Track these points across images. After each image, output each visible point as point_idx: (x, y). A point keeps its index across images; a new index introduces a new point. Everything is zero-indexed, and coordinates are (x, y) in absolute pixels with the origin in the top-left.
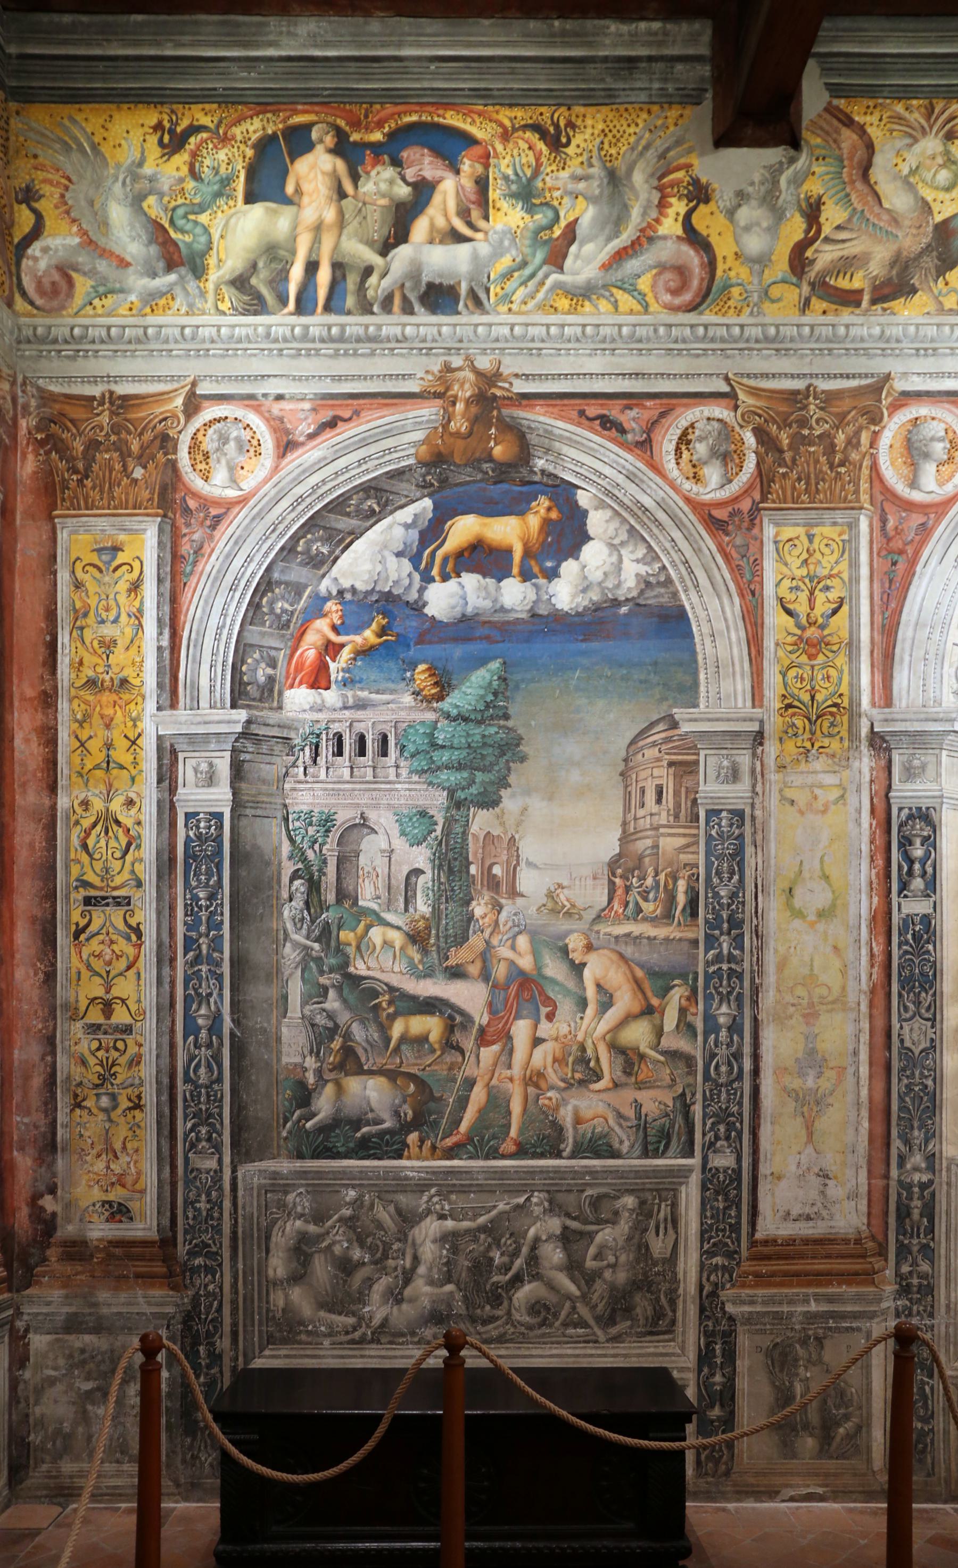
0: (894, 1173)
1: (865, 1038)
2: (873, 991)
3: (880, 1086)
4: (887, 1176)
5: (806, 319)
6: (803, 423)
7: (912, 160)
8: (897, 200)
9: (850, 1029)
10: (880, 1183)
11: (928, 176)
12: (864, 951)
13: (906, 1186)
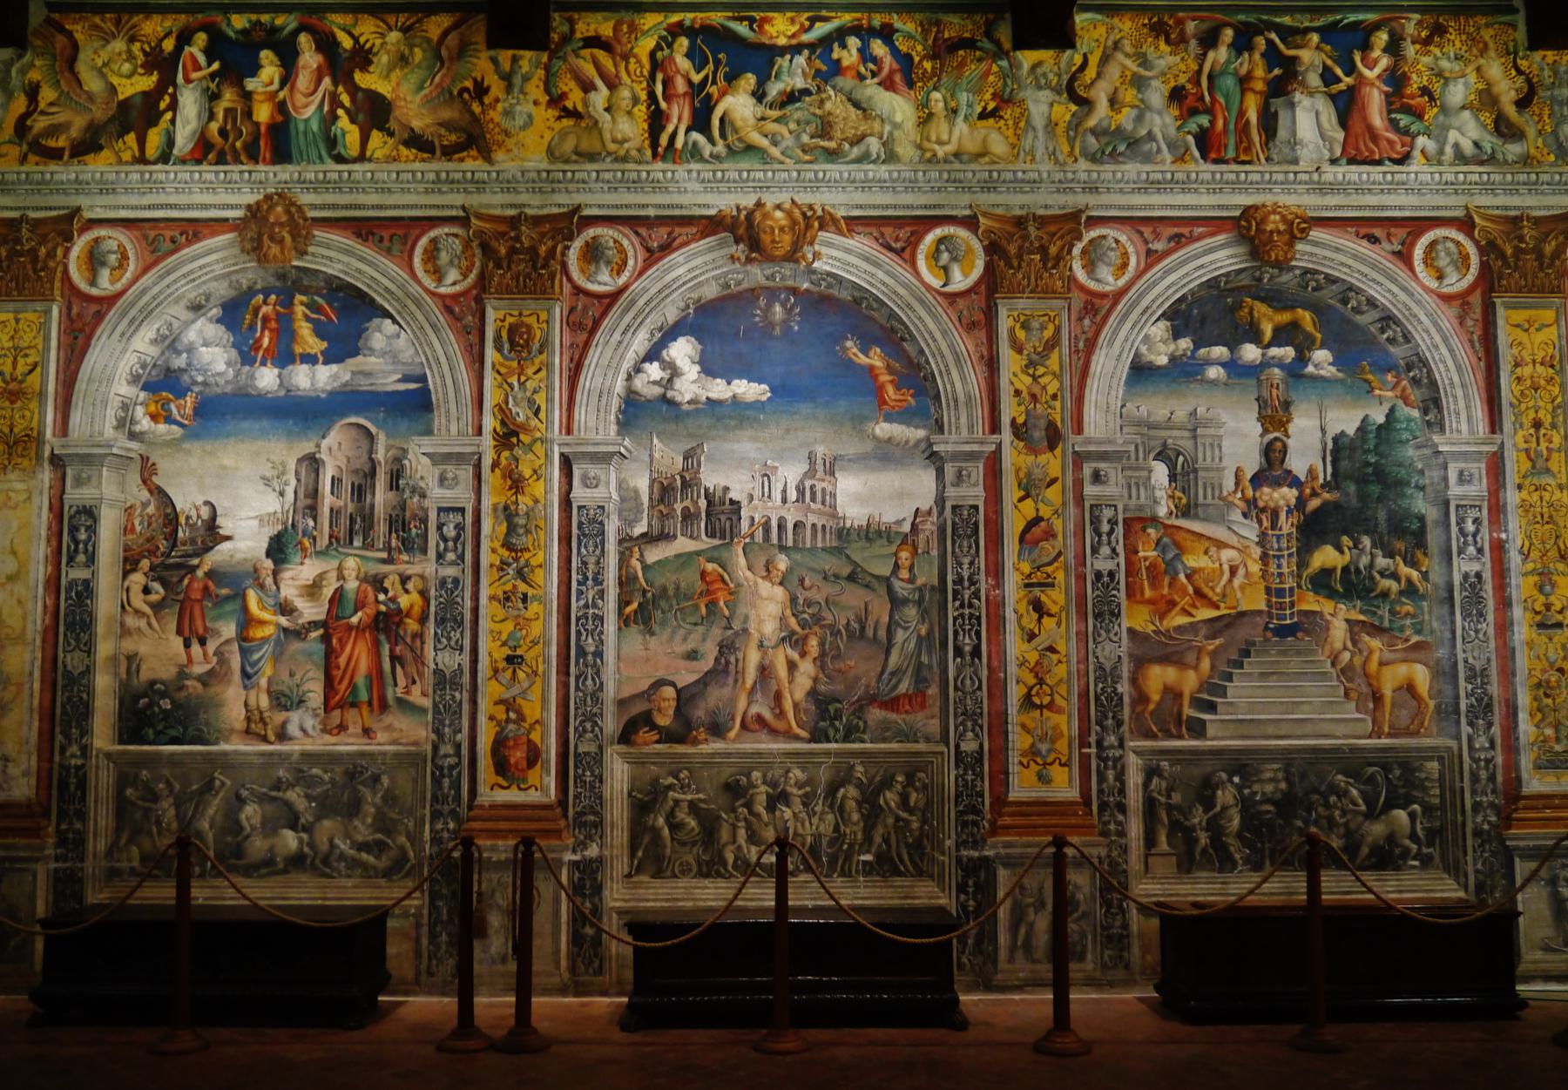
0: (57, 758)
1: (38, 663)
2: (45, 631)
3: (48, 695)
4: (51, 760)
5: (24, 169)
6: (18, 241)
7: (104, 56)
8: (93, 84)
9: (27, 657)
10: (46, 765)
11: (115, 67)
12: (40, 604)
13: (65, 768)
